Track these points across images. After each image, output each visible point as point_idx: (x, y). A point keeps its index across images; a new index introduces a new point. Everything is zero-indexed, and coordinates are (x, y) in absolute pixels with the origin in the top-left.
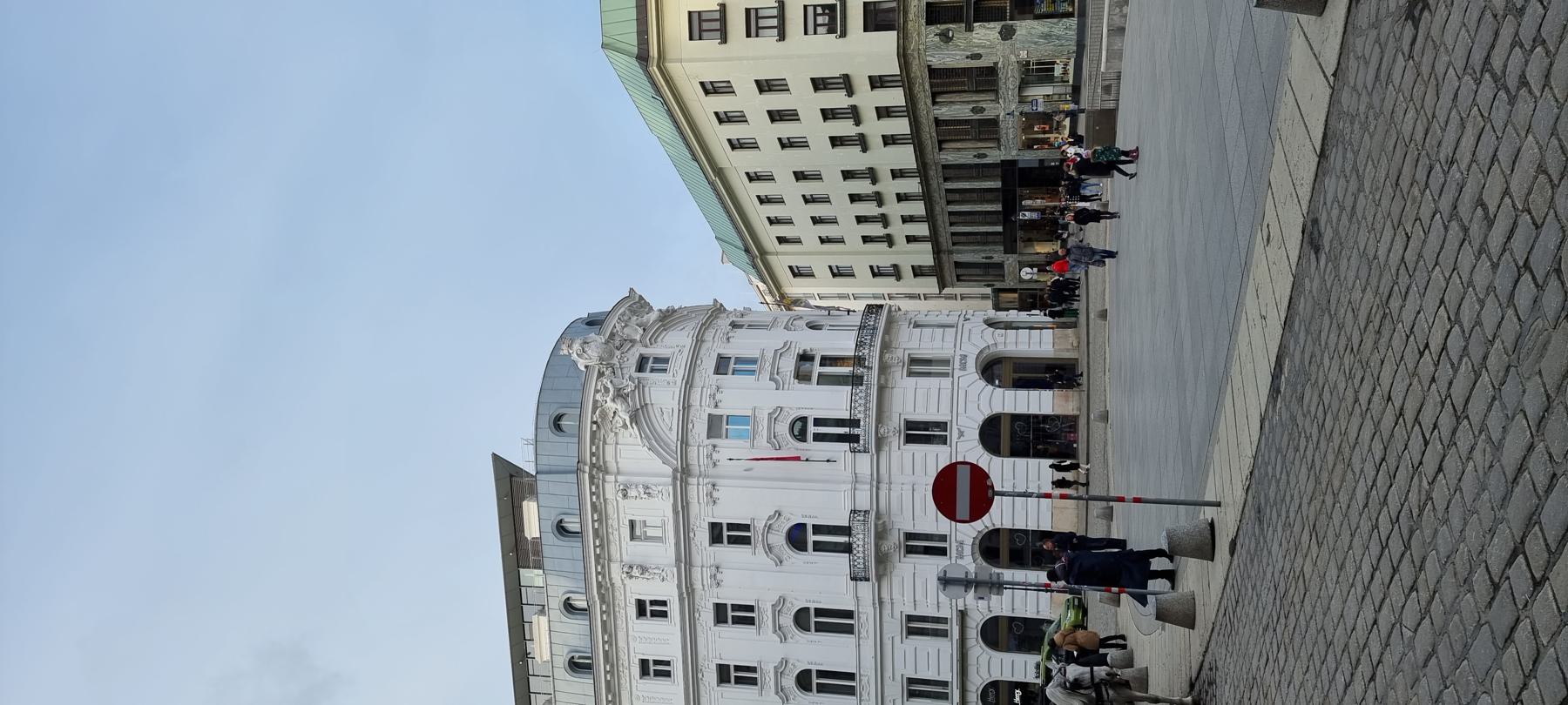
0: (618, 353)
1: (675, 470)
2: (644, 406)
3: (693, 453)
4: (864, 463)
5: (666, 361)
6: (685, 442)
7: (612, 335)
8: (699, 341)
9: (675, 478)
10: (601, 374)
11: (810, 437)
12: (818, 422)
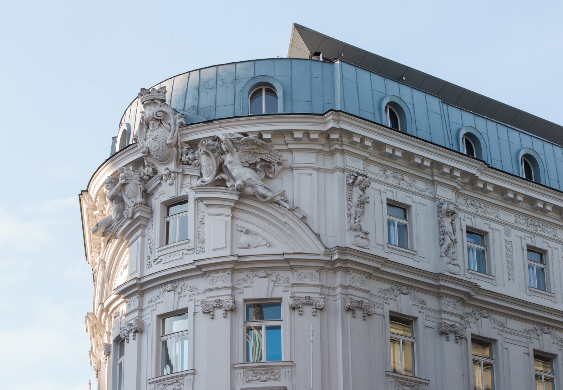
0: (172, 167)
7: (193, 145)
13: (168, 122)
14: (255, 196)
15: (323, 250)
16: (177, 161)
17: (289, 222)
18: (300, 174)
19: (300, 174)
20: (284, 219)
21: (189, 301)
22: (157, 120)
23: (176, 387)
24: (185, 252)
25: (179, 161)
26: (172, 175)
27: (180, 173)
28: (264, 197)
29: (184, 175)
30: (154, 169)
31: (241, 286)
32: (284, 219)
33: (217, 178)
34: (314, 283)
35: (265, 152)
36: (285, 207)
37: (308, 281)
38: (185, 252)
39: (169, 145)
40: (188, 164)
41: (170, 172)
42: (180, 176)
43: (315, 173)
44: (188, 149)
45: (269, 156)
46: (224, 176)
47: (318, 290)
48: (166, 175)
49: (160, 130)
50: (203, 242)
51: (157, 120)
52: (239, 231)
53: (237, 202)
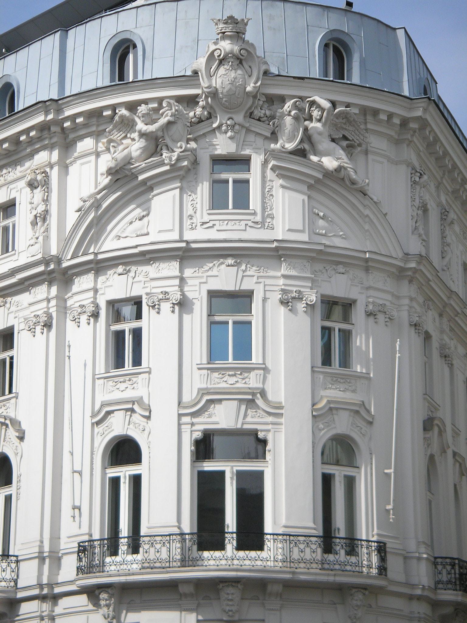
0: (239, 118)
1: (58, 260)
2: (148, 187)
3: (84, 282)
4: (69, 568)
5: (242, 201)
6: (99, 267)
8: (278, 253)
9: (46, 261)
10: (191, 101)
11: (113, 472)
12: (136, 480)
13: (250, 64)
14: (343, 179)
15: (400, 255)
16: (246, 113)
17: (372, 216)
18: (373, 160)
19: (373, 160)
20: (367, 212)
21: (256, 283)
22: (238, 59)
23: (129, 386)
24: (250, 223)
25: (248, 114)
26: (237, 127)
27: (245, 127)
28: (353, 183)
29: (248, 130)
30: (210, 113)
31: (320, 279)
32: (367, 212)
33: (299, 147)
34: (385, 288)
35: (351, 128)
36: (372, 199)
37: (380, 285)
38: (250, 223)
39: (248, 94)
40: (259, 120)
41: (235, 123)
42: (244, 131)
43: (385, 161)
44: (263, 101)
45: (353, 133)
46: (307, 146)
47: (389, 297)
48: (228, 126)
49: (239, 72)
50: (273, 218)
51: (238, 59)
52: (315, 213)
53: (318, 181)
